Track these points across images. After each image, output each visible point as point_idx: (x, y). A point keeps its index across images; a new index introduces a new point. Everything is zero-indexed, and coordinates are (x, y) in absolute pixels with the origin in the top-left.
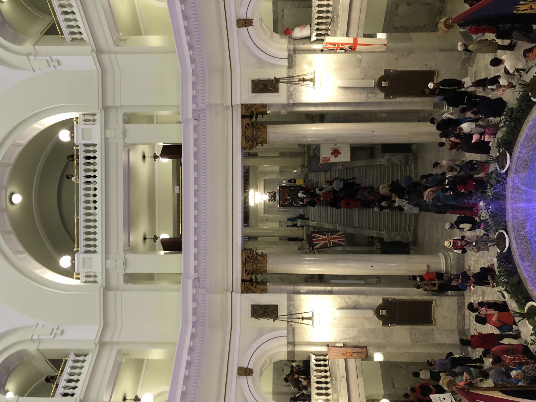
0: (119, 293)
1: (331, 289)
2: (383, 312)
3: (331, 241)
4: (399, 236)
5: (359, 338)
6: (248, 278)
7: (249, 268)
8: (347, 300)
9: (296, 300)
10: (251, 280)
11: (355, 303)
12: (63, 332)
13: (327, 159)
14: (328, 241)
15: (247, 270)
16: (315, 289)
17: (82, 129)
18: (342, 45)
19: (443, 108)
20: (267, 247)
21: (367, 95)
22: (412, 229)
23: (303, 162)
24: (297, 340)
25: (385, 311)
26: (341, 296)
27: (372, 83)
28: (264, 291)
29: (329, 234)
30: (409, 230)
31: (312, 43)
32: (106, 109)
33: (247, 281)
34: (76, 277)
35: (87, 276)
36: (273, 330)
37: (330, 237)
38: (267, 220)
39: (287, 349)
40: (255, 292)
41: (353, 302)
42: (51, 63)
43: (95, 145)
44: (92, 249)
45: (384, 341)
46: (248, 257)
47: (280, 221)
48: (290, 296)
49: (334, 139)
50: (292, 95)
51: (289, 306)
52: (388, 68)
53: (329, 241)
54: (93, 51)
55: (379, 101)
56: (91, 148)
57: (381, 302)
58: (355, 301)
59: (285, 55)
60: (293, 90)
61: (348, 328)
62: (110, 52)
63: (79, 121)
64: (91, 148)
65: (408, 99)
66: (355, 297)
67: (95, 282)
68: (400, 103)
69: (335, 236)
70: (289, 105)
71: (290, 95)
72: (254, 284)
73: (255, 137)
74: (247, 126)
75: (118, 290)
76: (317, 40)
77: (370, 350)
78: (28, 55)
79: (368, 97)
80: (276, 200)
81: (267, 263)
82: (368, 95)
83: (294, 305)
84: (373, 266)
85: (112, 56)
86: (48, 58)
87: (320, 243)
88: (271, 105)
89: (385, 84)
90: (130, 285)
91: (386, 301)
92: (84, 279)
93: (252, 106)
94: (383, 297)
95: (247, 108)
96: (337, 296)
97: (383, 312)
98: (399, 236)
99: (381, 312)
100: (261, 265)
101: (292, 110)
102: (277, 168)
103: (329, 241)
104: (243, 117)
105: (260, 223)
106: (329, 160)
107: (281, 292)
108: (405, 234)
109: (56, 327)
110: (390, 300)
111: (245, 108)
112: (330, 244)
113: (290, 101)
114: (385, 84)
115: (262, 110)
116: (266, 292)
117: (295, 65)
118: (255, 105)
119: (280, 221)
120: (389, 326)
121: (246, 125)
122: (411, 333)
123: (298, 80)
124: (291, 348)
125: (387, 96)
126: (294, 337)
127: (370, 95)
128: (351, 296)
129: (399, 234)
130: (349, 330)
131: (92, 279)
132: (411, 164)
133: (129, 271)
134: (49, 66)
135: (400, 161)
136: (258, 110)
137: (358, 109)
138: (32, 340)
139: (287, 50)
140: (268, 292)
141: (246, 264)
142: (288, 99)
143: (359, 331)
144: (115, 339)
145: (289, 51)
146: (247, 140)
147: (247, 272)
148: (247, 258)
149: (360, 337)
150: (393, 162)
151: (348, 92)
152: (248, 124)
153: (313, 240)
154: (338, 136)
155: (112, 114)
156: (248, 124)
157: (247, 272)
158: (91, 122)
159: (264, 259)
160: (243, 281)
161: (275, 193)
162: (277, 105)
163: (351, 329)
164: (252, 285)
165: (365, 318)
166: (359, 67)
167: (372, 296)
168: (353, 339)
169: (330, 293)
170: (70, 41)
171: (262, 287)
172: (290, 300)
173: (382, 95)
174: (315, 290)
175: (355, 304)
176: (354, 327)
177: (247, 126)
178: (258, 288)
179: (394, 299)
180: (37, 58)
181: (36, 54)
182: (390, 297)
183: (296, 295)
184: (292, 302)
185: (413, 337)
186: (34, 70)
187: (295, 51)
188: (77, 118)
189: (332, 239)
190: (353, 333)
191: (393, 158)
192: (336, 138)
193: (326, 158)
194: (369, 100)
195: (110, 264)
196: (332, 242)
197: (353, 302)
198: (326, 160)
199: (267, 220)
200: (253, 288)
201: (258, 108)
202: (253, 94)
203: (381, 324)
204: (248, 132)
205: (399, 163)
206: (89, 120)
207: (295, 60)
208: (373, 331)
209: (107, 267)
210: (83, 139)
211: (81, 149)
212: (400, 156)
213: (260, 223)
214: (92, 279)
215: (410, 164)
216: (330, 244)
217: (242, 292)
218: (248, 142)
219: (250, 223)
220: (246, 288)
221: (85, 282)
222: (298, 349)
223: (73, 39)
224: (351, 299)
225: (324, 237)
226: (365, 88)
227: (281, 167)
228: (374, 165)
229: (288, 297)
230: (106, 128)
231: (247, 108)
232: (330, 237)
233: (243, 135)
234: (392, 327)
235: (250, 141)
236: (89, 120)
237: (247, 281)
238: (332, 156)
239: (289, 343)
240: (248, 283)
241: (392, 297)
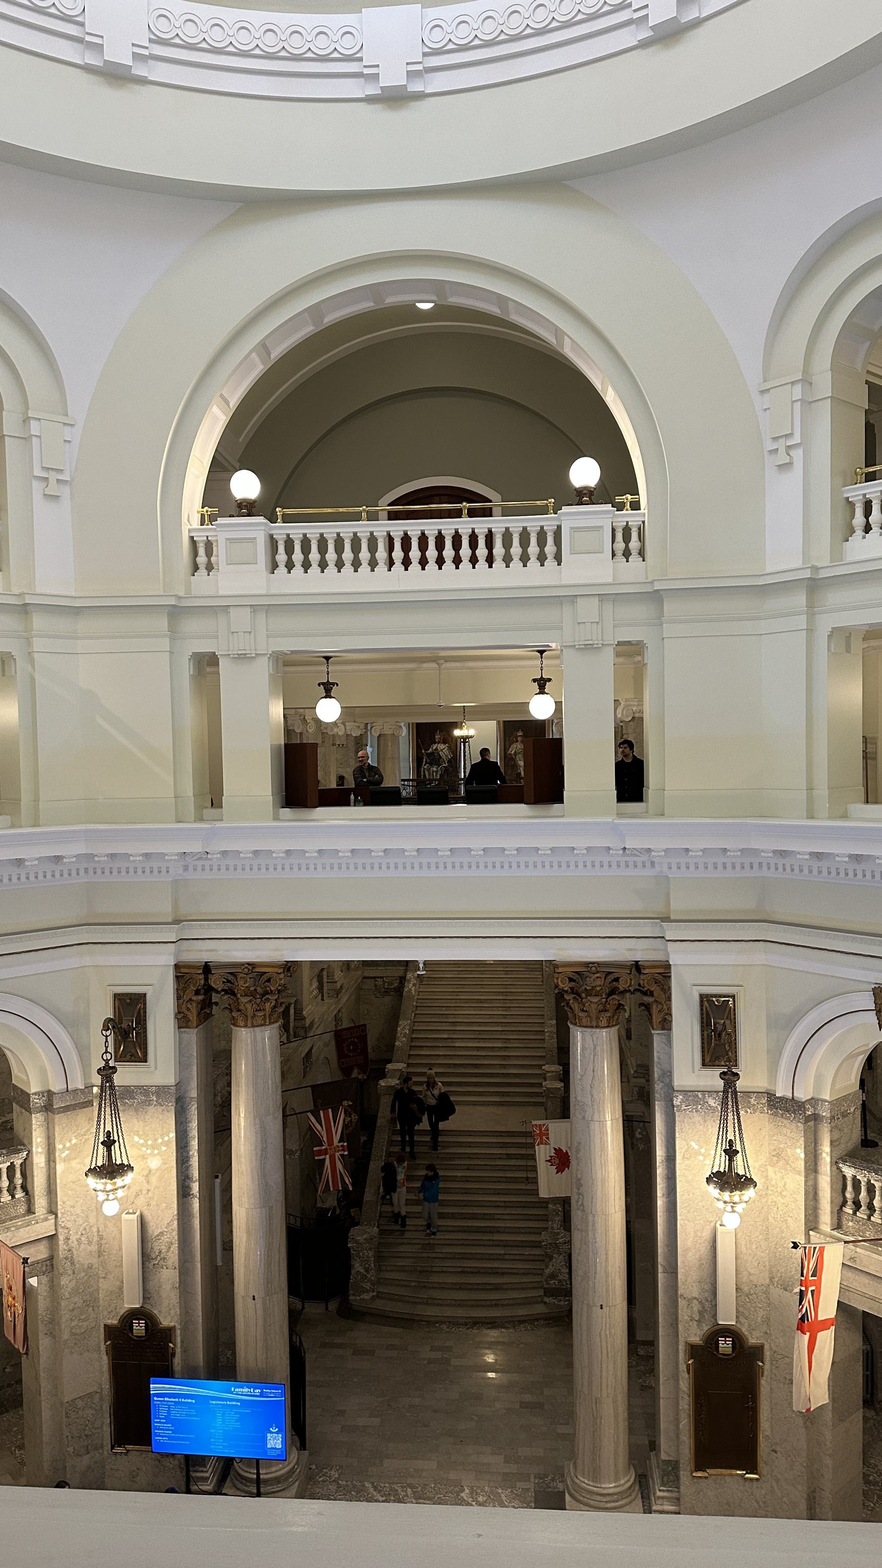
0: (165, 644)
1: (193, 1194)
2: (139, 1327)
3: (328, 1156)
4: (362, 1271)
5: (70, 1272)
6: (216, 982)
7: (242, 984)
8: (165, 1239)
9: (160, 1109)
10: (208, 989)
11: (159, 1258)
12: (55, 498)
13: (544, 1138)
14: (326, 1149)
15: (235, 976)
16: (191, 1153)
17: (602, 527)
18: (812, 1291)
19: (663, 1485)
21: (695, 1298)
22: (379, 1304)
24: (60, 1120)
25: (143, 1333)
26: (176, 1223)
27: (727, 1318)
28: (182, 1021)
29: (343, 1150)
30: (379, 1296)
31: (835, 1163)
32: (656, 597)
33: (206, 979)
34: (206, 513)
35: (209, 546)
36: (83, 1052)
37: (337, 1154)
39: (35, 1094)
40: (179, 998)
41: (160, 1252)
42: (781, 445)
43: (558, 558)
44: (282, 557)
45: (66, 1336)
46: (269, 980)
48: (170, 1093)
49: (582, 1204)
50: (697, 1103)
51: (144, 1090)
52: (767, 1354)
53: (325, 1152)
54: (815, 569)
55: (680, 1327)
56: (550, 548)
57: (166, 1321)
58: (164, 1258)
59: (802, 1095)
60: (710, 1106)
61: (96, 1239)
62: (811, 610)
63: (624, 512)
64: (550, 548)
65: (686, 1403)
66: (173, 1256)
67: (196, 568)
68: (676, 1377)
69: (339, 1166)
70: (670, 1091)
71: (693, 1096)
72: (201, 997)
73: (583, 995)
74: (612, 977)
75: (172, 639)
76: (844, 1177)
77: (50, 1275)
78: (806, 381)
79: (690, 1301)
81: (256, 1029)
82: (695, 1301)
83: (149, 1103)
84: (254, 1299)
85: (802, 621)
86: (797, 439)
87: (322, 1126)
88: (669, 1041)
89: (725, 1345)
90: (186, 669)
91: (169, 1332)
92: (200, 538)
93: (667, 991)
94: (178, 1327)
95: (660, 978)
96: (176, 1213)
97: (139, 1327)
99: (139, 1323)
100: (250, 1012)
101: (657, 1095)
103: (325, 1152)
104: (637, 966)
106: (541, 1143)
107: (182, 1065)
108: (368, 1286)
109: (66, 477)
110: (171, 1345)
111: (659, 973)
112: (320, 1153)
113: (681, 1097)
114: (725, 1345)
115: (656, 1018)
116: (179, 1028)
117: (775, 1115)
118: (669, 999)
120: (106, 1342)
121: (616, 975)
122: (90, 1395)
123: (730, 1136)
124: (37, 1101)
125: (693, 1350)
126: (66, 1109)
127: (696, 1306)
128: (175, 1247)
129: (367, 1270)
130: (90, 1243)
131: (202, 559)
133: (224, 665)
134: (775, 439)
135: (552, 1276)
136: (654, 1007)
137: (660, 1269)
138: (26, 420)
139: (816, 1096)
140: (180, 1033)
141: (250, 976)
142: (685, 1092)
143: (90, 1267)
144: (38, 644)
145: (814, 1101)
146: (576, 977)
147: (230, 978)
148: (265, 977)
149: (74, 1273)
150: (551, 1258)
151: (704, 1249)
152: (617, 980)
153: (330, 1110)
154: (590, 1218)
155: (640, 611)
156: (617, 980)
157: (230, 978)
158: (620, 545)
159: (265, 1019)
160: (207, 968)
162: (670, 1056)
163: (94, 1248)
164: (197, 993)
165: (121, 1288)
166: (771, 1279)
167: (178, 1301)
168: (66, 1258)
169: (184, 1192)
170: (846, 496)
171: (193, 1016)
172: (161, 1091)
173: (696, 1338)
174: (188, 1152)
175: (156, 1258)
176: (100, 1254)
177: (612, 977)
178: (189, 1006)
179: (173, 1355)
180: (798, 406)
181: (807, 403)
182: (179, 1345)
183: (173, 1108)
184: (155, 1099)
185: (80, 1404)
186: (762, 392)
187: (816, 1117)
188: (636, 506)
189: (332, 1158)
190: (84, 1254)
192: (583, 1211)
193: (548, 1134)
194: (681, 1303)
195: (241, 619)
196: (324, 1160)
197: (160, 1252)
198: (541, 1135)
200: (190, 994)
201: (660, 1007)
202: (697, 998)
203: (109, 1322)
204: (596, 981)
205: (547, 1271)
206: (627, 538)
207: (788, 1119)
208: (92, 1302)
209: (231, 610)
210: (574, 530)
211: (548, 521)
214: (202, 559)
215: (546, 1299)
216: (320, 1153)
217: (177, 967)
218: (571, 980)
220: (188, 976)
221: (193, 542)
222: (37, 1120)
223: (851, 505)
224: (170, 1248)
225: (336, 1138)
226: (715, 1294)
229: (168, 1087)
230: (602, 598)
231: (660, 978)
232: (337, 1154)
233: (587, 964)
234: (103, 1347)
235: (573, 984)
236: (627, 538)
237: (206, 979)
238: (553, 1151)
239: (50, 1094)
240: (202, 982)
241: (178, 1350)
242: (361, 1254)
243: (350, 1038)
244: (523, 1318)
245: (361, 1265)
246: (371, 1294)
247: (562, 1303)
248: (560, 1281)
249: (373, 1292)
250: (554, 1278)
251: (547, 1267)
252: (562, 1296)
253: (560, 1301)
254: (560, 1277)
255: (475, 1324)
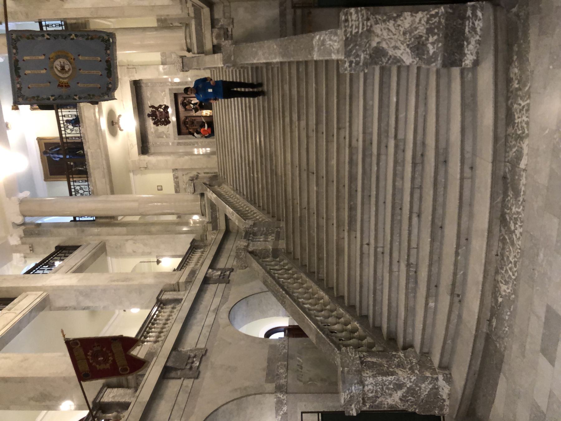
4: (400, 393)
20: (127, 240)
23: (188, 41)
30: (445, 367)
38: (146, 168)
47: (175, 170)
80: (169, 122)
98: (400, 393)
102: (156, 57)
105: (131, 175)
119: (175, 170)
129: (399, 386)
132: (476, 63)
161: (166, 107)
191: (377, 29)
199: (146, 168)
205: (408, 59)
212: (420, 15)
213: (131, 175)
215: (468, 61)
219: (92, 186)
227: (163, 55)
228: (306, 63)
242: (370, 395)
243: (88, 360)
244: (502, 115)
245: (391, 395)
246: (441, 382)
247: (479, 25)
248: (430, 31)
249: (437, 379)
250: (424, 45)
251: (398, 61)
252: (463, 25)
253: (474, 29)
254: (422, 30)
255: (504, 222)
